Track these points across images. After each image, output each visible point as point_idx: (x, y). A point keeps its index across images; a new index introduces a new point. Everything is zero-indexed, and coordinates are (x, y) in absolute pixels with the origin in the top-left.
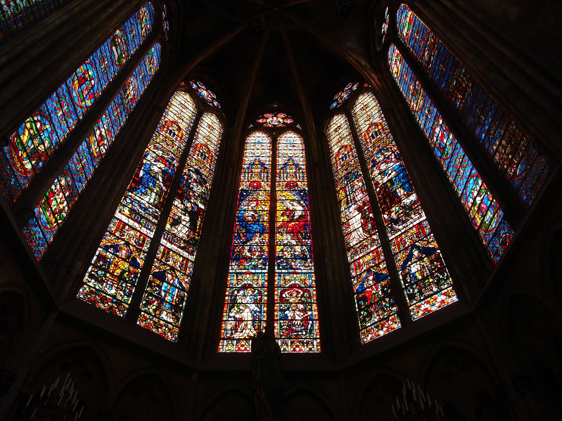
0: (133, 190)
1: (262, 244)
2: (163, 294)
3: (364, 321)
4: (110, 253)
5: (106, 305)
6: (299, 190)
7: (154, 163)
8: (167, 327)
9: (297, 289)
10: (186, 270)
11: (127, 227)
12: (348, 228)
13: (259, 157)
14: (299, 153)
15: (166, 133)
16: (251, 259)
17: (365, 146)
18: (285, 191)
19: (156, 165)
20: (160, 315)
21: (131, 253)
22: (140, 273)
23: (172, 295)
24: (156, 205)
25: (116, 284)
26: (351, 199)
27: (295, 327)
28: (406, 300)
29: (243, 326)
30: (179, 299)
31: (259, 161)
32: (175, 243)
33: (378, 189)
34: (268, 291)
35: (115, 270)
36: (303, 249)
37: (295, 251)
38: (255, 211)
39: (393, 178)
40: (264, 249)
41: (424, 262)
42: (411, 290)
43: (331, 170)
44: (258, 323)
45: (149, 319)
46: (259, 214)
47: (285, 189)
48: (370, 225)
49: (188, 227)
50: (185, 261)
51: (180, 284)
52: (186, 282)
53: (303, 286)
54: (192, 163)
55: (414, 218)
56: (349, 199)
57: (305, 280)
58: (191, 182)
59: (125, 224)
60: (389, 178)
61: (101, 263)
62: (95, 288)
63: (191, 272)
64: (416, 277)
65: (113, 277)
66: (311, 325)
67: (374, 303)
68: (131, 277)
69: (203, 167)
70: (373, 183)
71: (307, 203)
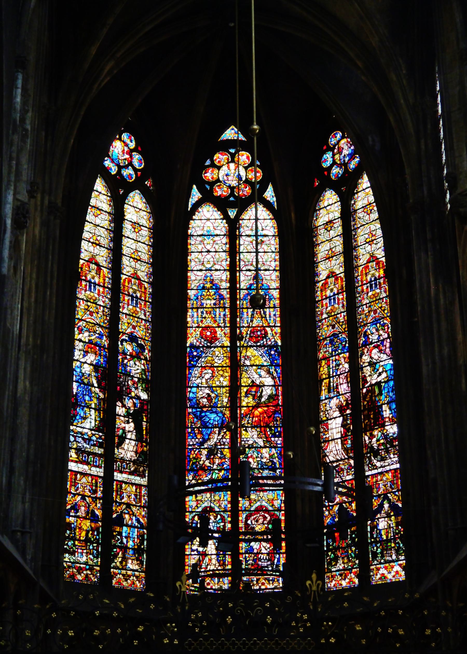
0: (73, 420)
1: (223, 447)
2: (125, 540)
3: (330, 564)
4: (72, 516)
5: (82, 574)
6: (269, 346)
7: (83, 360)
8: (134, 575)
9: (263, 514)
10: (140, 501)
11: (78, 476)
12: (326, 431)
13: (211, 270)
14: (270, 260)
15: (86, 291)
16: (211, 470)
17: (360, 296)
18: (251, 346)
19: (85, 363)
20: (126, 565)
21: (89, 506)
22: (102, 526)
23: (133, 538)
24: (98, 426)
25: (84, 549)
26: (333, 387)
27: (261, 561)
28: (369, 557)
29: (207, 561)
30: (140, 540)
31: (212, 281)
32: (125, 470)
33: (365, 390)
34: (232, 516)
35: (80, 534)
36: (272, 453)
37: (262, 458)
38: (210, 387)
39: (383, 382)
40: (225, 453)
41: (391, 521)
42: (375, 548)
43: (313, 314)
44: (223, 557)
45: (118, 573)
46: (216, 393)
47: (250, 344)
48: (349, 442)
49: (134, 440)
50: (138, 490)
51: (138, 521)
52: (143, 517)
53: (270, 508)
54: (123, 327)
55: (392, 459)
56: (332, 384)
57: (273, 500)
58: (127, 362)
59: (77, 473)
60: (379, 379)
61: (68, 532)
62: (70, 562)
63: (146, 501)
64: (381, 535)
65: (80, 543)
66: (278, 559)
67: (342, 548)
68: (95, 535)
69: (137, 322)
70: (360, 375)
71: (279, 371)
